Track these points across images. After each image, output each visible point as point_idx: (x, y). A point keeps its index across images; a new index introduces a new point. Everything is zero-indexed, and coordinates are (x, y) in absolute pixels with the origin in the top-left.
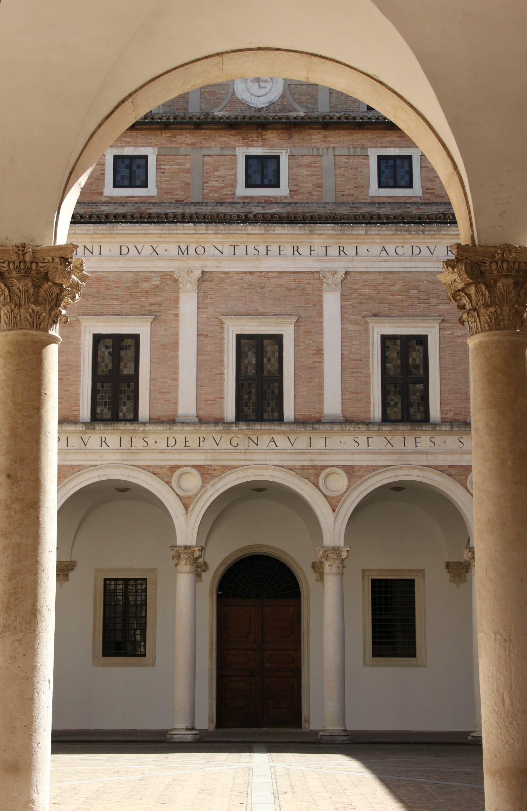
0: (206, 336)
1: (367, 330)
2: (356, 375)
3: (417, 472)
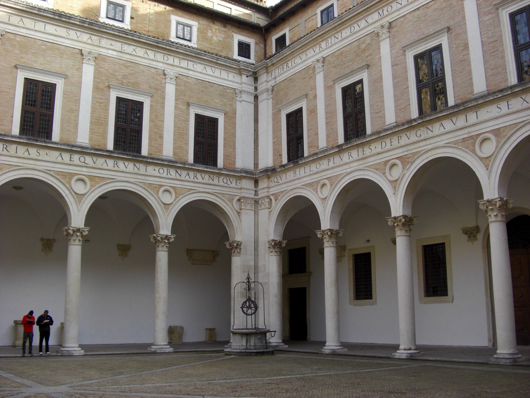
0: (397, 65)
2: (494, 54)
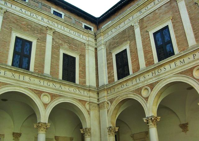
1: (11, 32)
3: (23, 89)
